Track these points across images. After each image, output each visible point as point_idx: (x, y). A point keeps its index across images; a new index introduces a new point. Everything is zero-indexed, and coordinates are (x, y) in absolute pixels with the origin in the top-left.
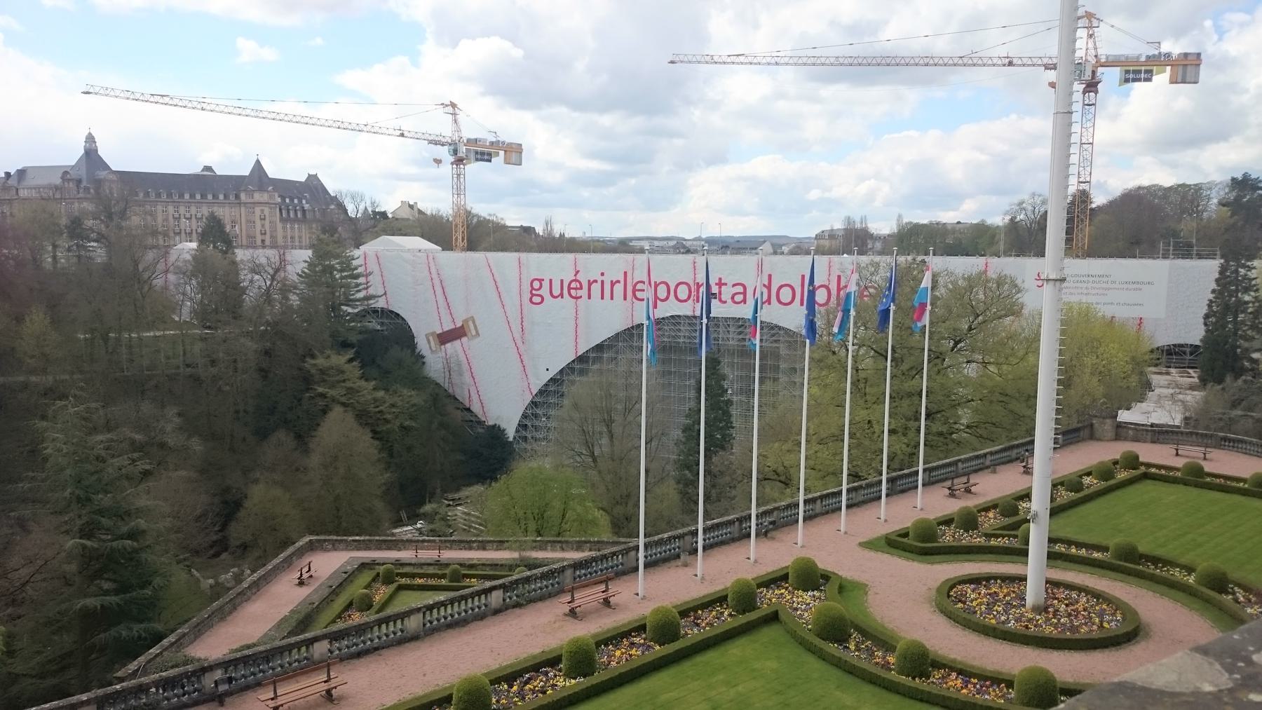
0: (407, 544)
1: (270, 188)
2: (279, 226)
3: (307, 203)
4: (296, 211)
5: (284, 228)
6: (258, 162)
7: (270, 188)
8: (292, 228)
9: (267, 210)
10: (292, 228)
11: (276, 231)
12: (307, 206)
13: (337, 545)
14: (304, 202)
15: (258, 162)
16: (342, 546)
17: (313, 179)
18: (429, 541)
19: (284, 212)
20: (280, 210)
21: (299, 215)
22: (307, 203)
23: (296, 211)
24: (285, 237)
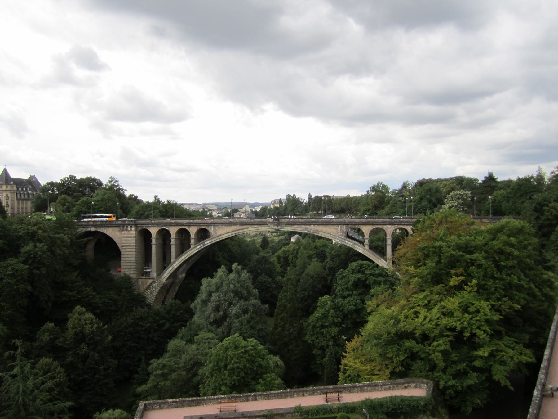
0: (208, 401)
1: (12, 183)
2: (16, 202)
3: (30, 190)
4: (21, 194)
5: (18, 204)
6: (5, 170)
7: (12, 183)
8: (22, 204)
9: (9, 195)
10: (22, 204)
11: (14, 205)
12: (30, 192)
13: (162, 406)
14: (28, 189)
15: (5, 170)
16: (166, 406)
17: (32, 177)
18: (221, 398)
19: (18, 195)
20: (17, 194)
21: (26, 197)
22: (30, 190)
23: (21, 194)
24: (18, 208)
